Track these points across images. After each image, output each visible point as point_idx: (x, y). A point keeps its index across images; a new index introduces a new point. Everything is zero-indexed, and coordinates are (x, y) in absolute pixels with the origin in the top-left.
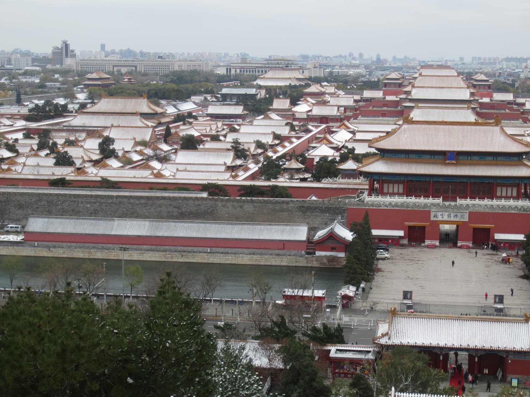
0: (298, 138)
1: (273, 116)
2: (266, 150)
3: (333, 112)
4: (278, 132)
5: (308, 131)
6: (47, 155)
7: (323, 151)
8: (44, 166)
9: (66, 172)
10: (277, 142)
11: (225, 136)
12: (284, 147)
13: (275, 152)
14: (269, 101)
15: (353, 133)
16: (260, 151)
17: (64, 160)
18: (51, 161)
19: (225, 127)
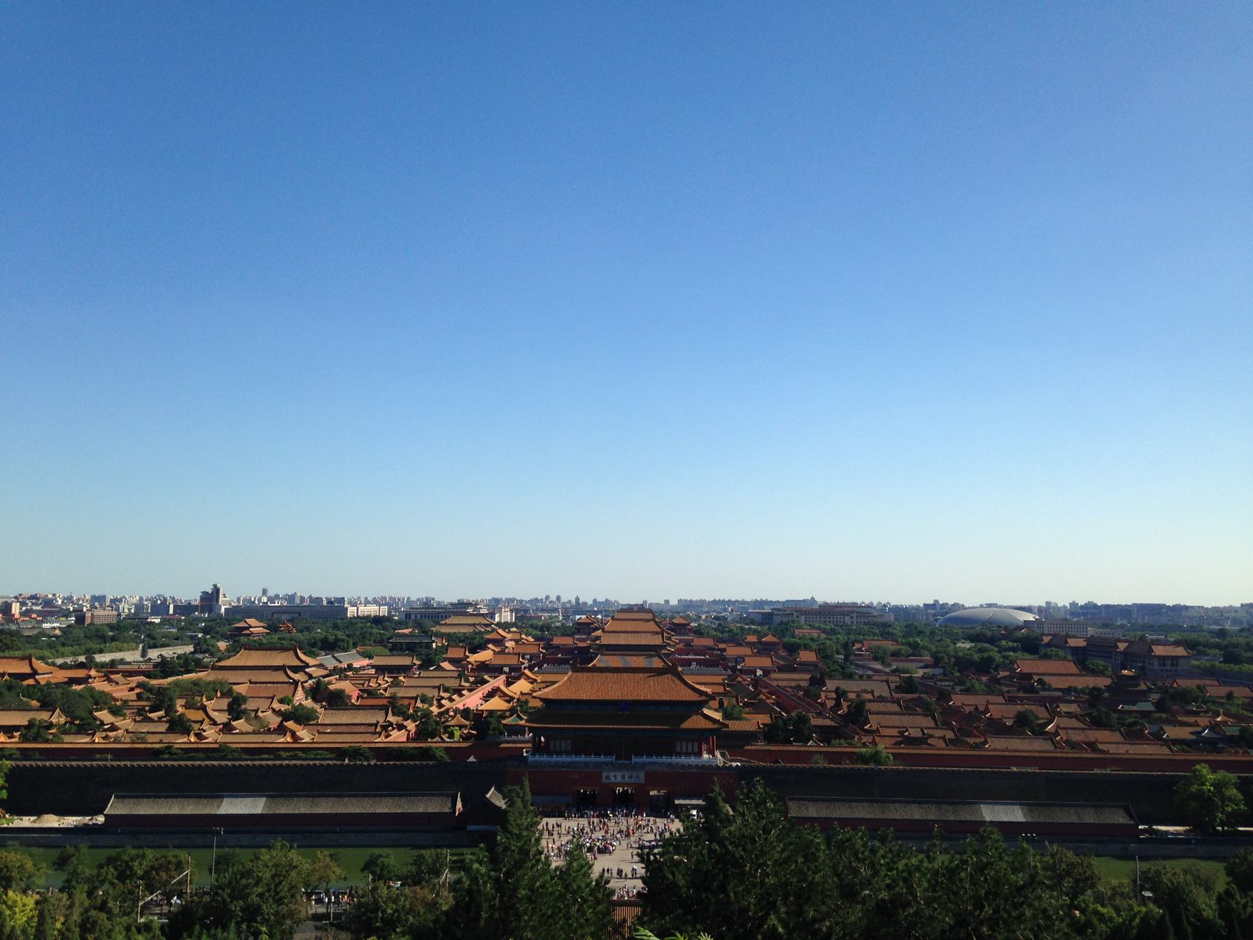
0: (470, 690)
1: (446, 665)
2: (431, 705)
3: (513, 661)
4: (447, 685)
5: (485, 682)
6: (160, 718)
7: (497, 704)
8: (155, 733)
9: (180, 741)
10: (446, 695)
11: (385, 690)
12: (451, 700)
13: (440, 706)
14: (444, 649)
15: (533, 681)
16: (426, 706)
17: (178, 725)
18: (163, 727)
19: (390, 680)
